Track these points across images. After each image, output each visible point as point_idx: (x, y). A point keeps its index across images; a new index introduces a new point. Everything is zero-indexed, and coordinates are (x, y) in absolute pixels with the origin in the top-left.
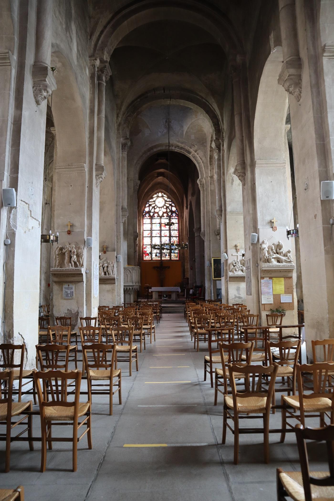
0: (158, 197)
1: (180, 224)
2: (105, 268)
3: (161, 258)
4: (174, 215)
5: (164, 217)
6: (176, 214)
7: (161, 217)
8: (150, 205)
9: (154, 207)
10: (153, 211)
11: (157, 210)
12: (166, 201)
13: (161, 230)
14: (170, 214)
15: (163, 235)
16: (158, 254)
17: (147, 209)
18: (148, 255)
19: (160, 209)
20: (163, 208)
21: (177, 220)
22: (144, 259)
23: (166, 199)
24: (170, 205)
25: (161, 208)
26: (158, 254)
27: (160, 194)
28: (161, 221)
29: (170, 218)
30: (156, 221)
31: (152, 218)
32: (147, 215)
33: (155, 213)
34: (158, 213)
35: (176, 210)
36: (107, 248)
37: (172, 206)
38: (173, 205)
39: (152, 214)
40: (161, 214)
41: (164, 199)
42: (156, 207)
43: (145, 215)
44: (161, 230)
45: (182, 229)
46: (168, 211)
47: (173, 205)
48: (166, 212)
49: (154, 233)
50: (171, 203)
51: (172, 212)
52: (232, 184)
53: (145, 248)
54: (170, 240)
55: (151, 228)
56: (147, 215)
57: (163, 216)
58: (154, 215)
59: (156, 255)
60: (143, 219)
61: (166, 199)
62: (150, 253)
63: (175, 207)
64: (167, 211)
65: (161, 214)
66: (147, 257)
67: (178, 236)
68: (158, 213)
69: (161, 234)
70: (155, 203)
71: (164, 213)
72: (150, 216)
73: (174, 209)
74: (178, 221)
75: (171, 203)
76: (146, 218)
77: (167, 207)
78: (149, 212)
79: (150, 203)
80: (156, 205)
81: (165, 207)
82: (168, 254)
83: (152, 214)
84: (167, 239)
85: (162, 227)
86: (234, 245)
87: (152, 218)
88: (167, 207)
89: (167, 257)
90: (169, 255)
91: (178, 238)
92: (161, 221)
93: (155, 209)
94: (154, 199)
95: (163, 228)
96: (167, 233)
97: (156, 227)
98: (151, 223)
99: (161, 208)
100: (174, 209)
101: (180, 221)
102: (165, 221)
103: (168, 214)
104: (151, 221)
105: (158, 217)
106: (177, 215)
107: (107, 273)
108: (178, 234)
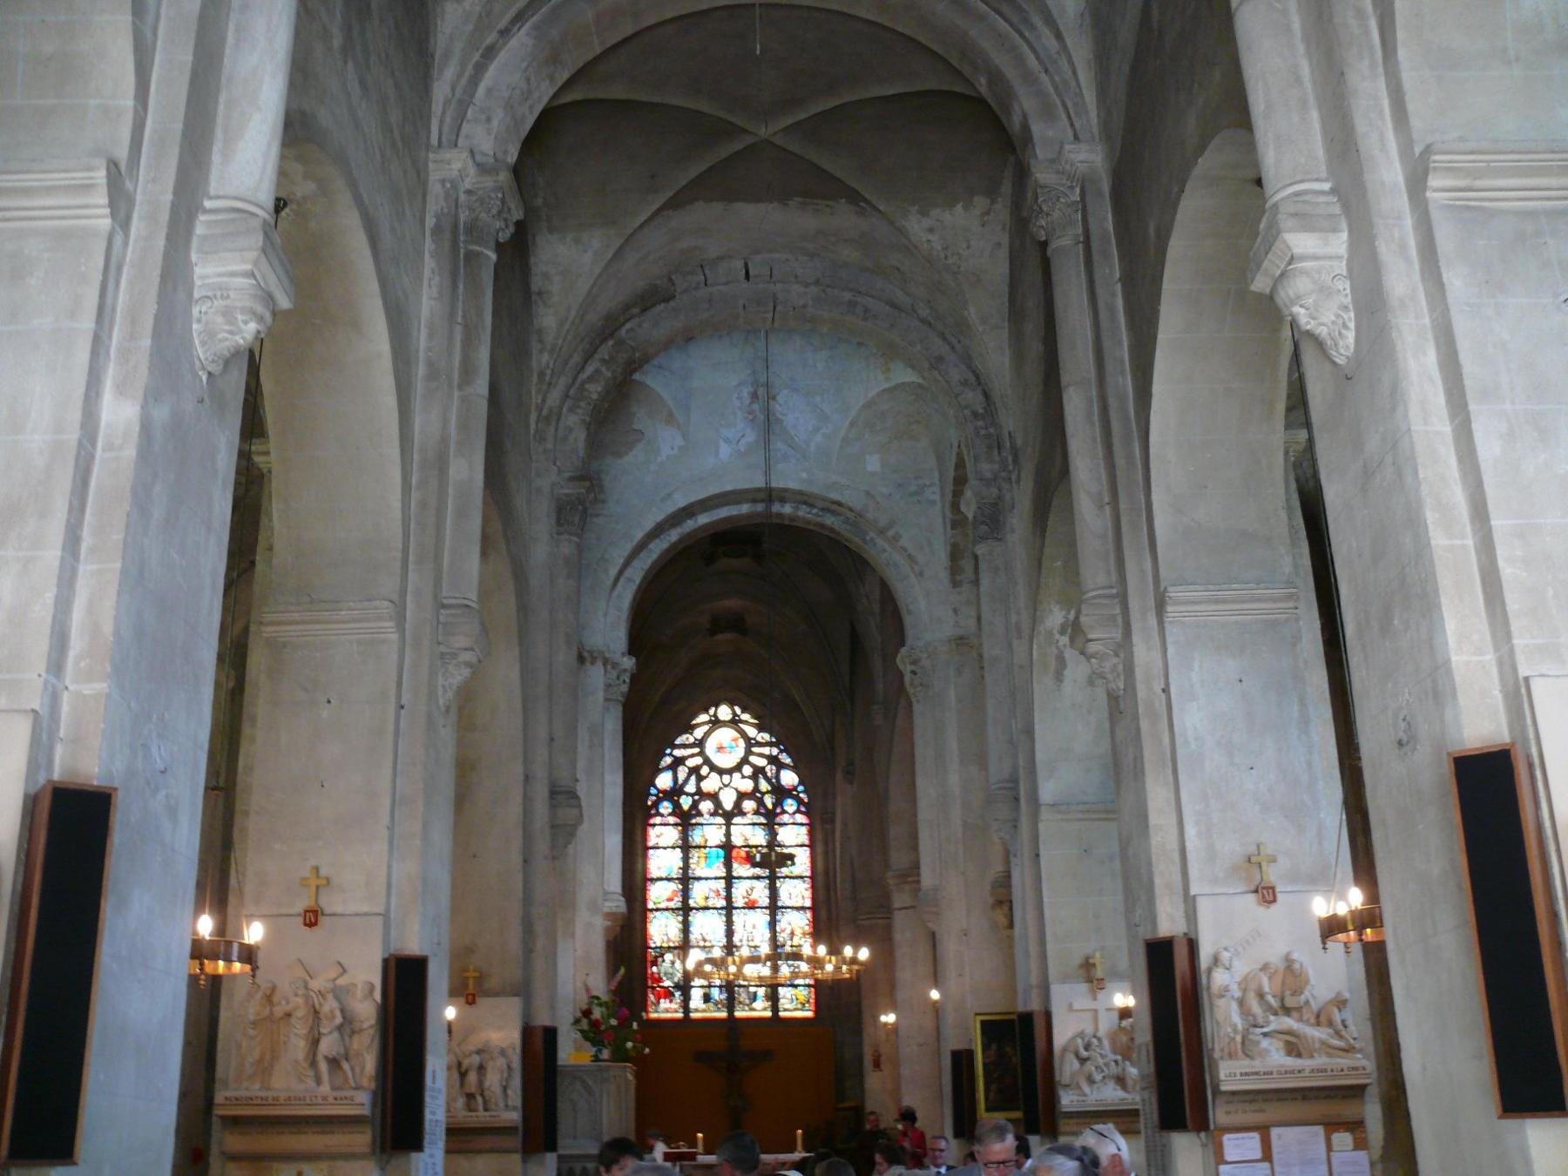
0: (716, 723)
1: (820, 848)
2: (472, 1077)
4: (790, 805)
5: (743, 814)
6: (800, 802)
7: (728, 817)
8: (679, 761)
9: (695, 770)
10: (691, 787)
11: (711, 783)
12: (750, 743)
13: (729, 879)
14: (769, 801)
15: (739, 901)
16: (715, 993)
17: (664, 781)
18: (669, 994)
19: (726, 778)
20: (736, 775)
21: (804, 830)
22: (653, 1015)
23: (752, 732)
24: (773, 760)
25: (730, 772)
26: (715, 993)
27: (724, 712)
28: (728, 834)
29: (771, 820)
30: (710, 833)
31: (686, 820)
32: (666, 807)
33: (701, 795)
34: (714, 797)
35: (800, 783)
36: (480, 979)
39: (686, 802)
41: (743, 734)
42: (705, 770)
43: (656, 805)
44: (729, 879)
45: (826, 873)
46: (764, 786)
49: (699, 893)
50: (775, 751)
51: (780, 793)
52: (1059, 677)
53: (655, 963)
55: (686, 867)
56: (666, 807)
57: (738, 810)
58: (695, 805)
59: (707, 998)
60: (646, 825)
61: (752, 732)
62: (677, 986)
63: (794, 769)
64: (756, 789)
66: (664, 1004)
68: (714, 797)
69: (729, 898)
70: (702, 754)
71: (742, 796)
72: (677, 810)
73: (789, 778)
74: (811, 834)
75: (775, 751)
76: (658, 820)
77: (758, 772)
78: (675, 793)
79: (677, 753)
80: (707, 761)
81: (747, 770)
83: (686, 802)
84: (761, 918)
85: (735, 865)
86: (1077, 960)
87: (686, 820)
88: (758, 772)
91: (809, 914)
92: (728, 834)
93: (700, 778)
94: (699, 733)
96: (761, 892)
97: (708, 867)
98: (686, 847)
99: (730, 772)
100: (789, 778)
101: (819, 836)
102: (748, 833)
103: (761, 802)
104: (685, 837)
105: (714, 814)
106: (808, 809)
107: (479, 1099)
108: (808, 894)
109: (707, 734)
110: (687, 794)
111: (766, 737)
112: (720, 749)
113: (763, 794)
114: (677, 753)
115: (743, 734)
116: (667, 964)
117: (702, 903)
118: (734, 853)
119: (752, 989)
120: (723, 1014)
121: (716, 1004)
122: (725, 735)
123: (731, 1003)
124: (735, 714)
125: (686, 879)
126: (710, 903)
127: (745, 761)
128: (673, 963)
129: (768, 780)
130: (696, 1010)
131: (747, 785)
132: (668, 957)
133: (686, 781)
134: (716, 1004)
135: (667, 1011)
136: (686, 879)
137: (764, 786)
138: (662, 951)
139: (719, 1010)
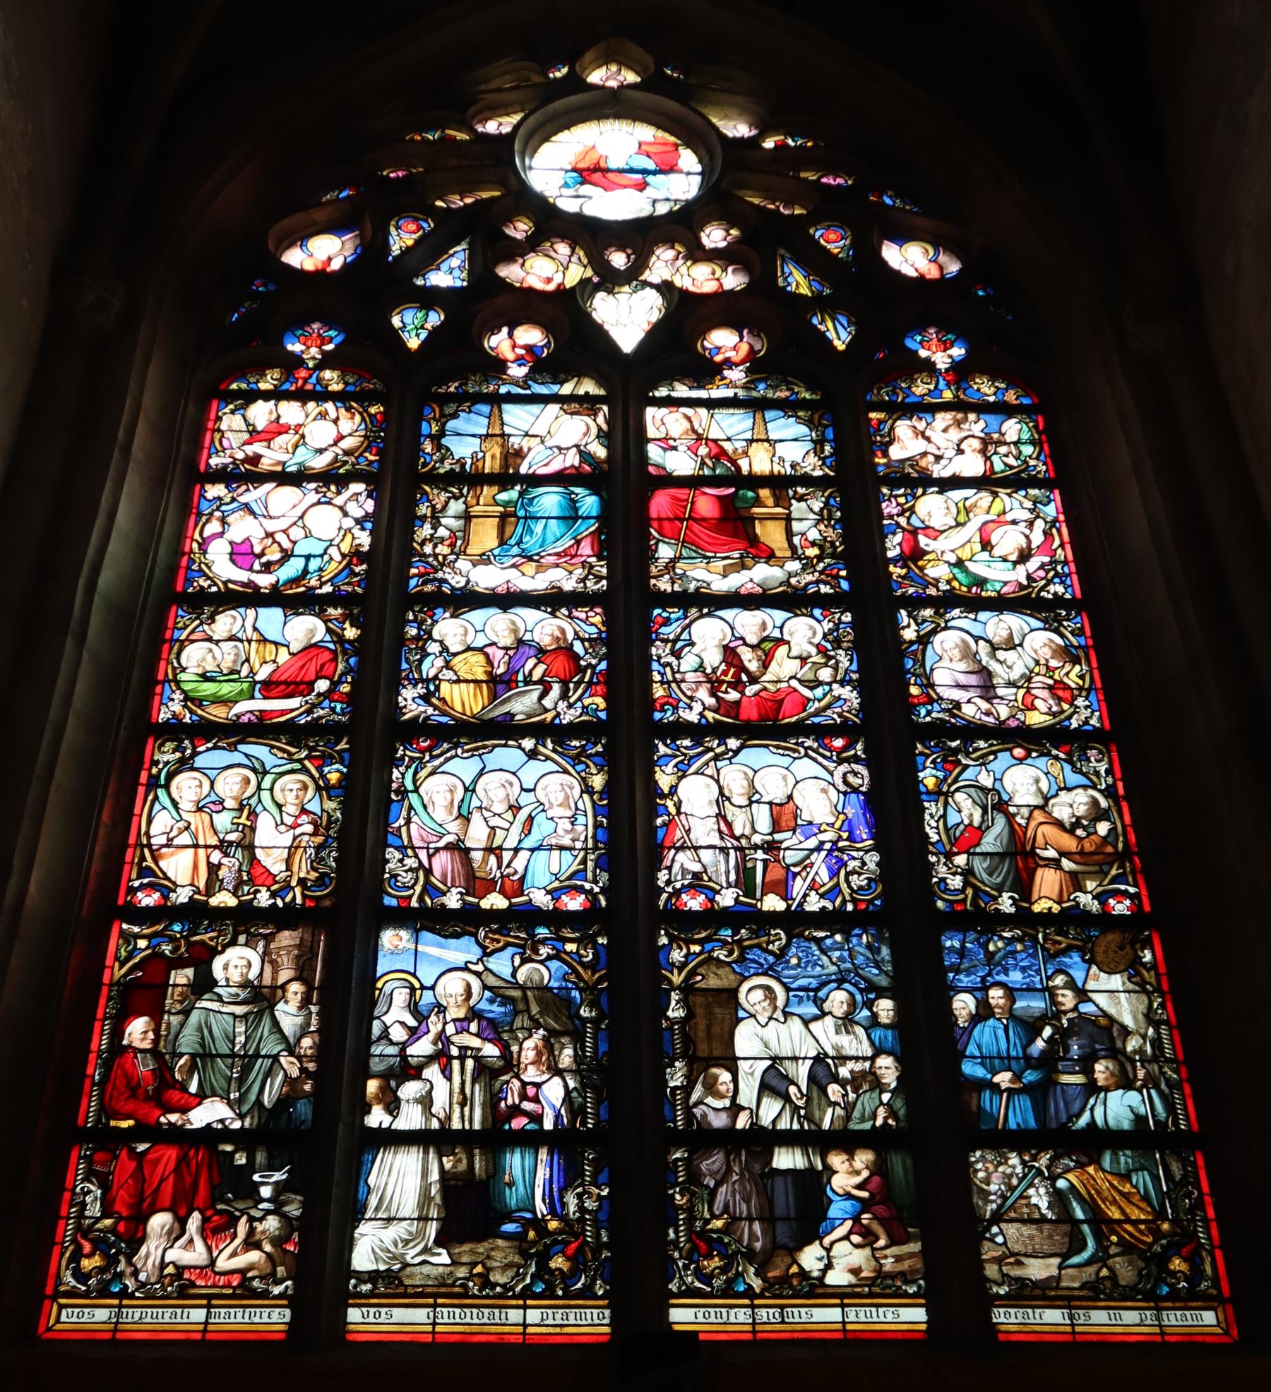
3: (639, 1301)
11: (544, 271)
16: (529, 1176)
26: (529, 1176)
31: (407, 394)
40: (627, 318)
53: (145, 993)
54: (892, 809)
59: (467, 1209)
62: (271, 1132)
66: (168, 1245)
67: (1086, 714)
82: (847, 1174)
87: (407, 394)
89: (840, 1257)
90: (885, 1209)
95: (682, 565)
116: (219, 1017)
117: (465, 700)
118: (660, 503)
119: (786, 1159)
120: (590, 1321)
121: (535, 1244)
123: (631, 1257)
125: (385, 600)
126: (522, 705)
128: (261, 998)
130: (390, 1284)
132: (236, 963)
134: (535, 1244)
135: (180, 1284)
136: (385, 600)
138: (200, 926)
139: (551, 1288)
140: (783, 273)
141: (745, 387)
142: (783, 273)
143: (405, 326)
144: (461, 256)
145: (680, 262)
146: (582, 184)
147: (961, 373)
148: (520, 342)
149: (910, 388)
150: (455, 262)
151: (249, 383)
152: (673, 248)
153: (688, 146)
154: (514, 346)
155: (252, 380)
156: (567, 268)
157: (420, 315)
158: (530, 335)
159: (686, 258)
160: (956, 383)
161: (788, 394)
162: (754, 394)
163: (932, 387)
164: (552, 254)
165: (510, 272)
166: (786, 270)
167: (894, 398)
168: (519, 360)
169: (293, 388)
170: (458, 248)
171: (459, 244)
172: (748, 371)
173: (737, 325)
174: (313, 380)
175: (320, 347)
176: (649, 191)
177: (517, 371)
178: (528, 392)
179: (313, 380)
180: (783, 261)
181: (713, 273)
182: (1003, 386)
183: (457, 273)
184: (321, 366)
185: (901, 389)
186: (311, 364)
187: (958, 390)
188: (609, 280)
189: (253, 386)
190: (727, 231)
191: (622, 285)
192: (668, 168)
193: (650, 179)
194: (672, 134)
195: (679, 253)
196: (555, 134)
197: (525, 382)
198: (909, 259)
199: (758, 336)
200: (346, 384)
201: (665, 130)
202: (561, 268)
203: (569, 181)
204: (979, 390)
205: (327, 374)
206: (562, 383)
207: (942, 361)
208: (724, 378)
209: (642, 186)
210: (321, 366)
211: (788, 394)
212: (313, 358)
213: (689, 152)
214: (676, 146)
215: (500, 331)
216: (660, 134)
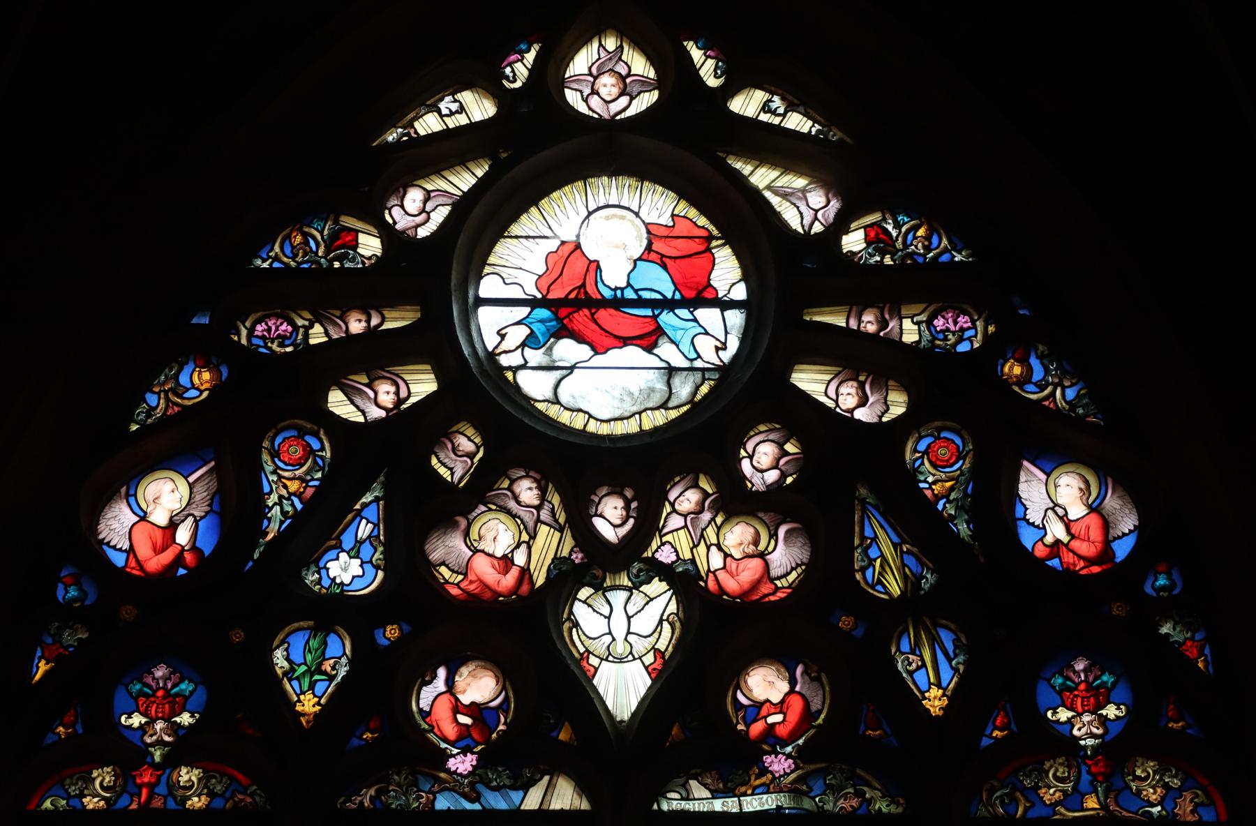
0: (541, 150)
11: (499, 544)
12: (791, 279)
23: (802, 204)
27: (606, 79)
33: (425, 619)
37: (1011, 440)
38: (1038, 381)
39: (309, 673)
40: (622, 644)
41: (747, 222)
42: (455, 461)
43: (92, 684)
46: (886, 564)
47: (1038, 381)
48: (817, 621)
50: (966, 332)
58: (380, 687)
61: (802, 204)
65: (622, 644)
68: (524, 631)
71: (716, 631)
75: (966, 332)
78: (246, 583)
79: (265, 333)
80: (480, 392)
88: (838, 479)
94: (420, 210)
99: (644, 463)
109: (480, 225)
110: (335, 610)
111: (916, 238)
112: (576, 307)
113: (890, 618)
114: (265, 333)
115: (747, 222)
122: (610, 226)
124: (675, 75)
127: (746, 393)
129: (915, 519)
131: (744, 555)
133: (319, 526)
137: (886, 564)
140: (863, 538)
141: (794, 791)
142: (863, 538)
143: (293, 670)
144: (371, 512)
145: (706, 516)
146: (558, 334)
147: (1118, 751)
148: (466, 699)
149: (1037, 788)
150: (364, 529)
151: (68, 797)
152: (695, 485)
153: (729, 240)
154: (457, 708)
155: (73, 790)
156: (533, 536)
157: (314, 644)
158: (479, 686)
159: (716, 508)
160: (1107, 778)
161: (855, 803)
162: (807, 804)
163: (1069, 786)
164: (512, 504)
165: (447, 549)
166: (868, 532)
167: (1011, 809)
168: (464, 741)
169: (134, 806)
170: (368, 498)
171: (368, 489)
172: (800, 757)
173: (785, 659)
174: (162, 789)
175: (167, 719)
176: (665, 350)
177: (462, 764)
178: (477, 806)
179: (162, 789)
180: (864, 511)
181: (756, 543)
182: (1176, 783)
183: (366, 551)
184: (175, 758)
185: (1024, 790)
186: (157, 755)
187: (1107, 793)
188: (596, 565)
189: (75, 802)
190: (780, 445)
191: (616, 571)
192: (699, 296)
193: (666, 319)
194: (703, 211)
195: (706, 495)
196: (515, 218)
197: (472, 785)
198: (1055, 504)
199: (817, 679)
200: (211, 794)
201: (692, 203)
202: (525, 537)
203: (539, 329)
204: (1139, 792)
205: (186, 775)
206: (526, 787)
207: (1085, 730)
208: (764, 771)
209: (650, 339)
210: (175, 758)
211: (855, 803)
212: (160, 742)
213: (727, 251)
214: (711, 238)
215: (434, 676)
216: (683, 208)
